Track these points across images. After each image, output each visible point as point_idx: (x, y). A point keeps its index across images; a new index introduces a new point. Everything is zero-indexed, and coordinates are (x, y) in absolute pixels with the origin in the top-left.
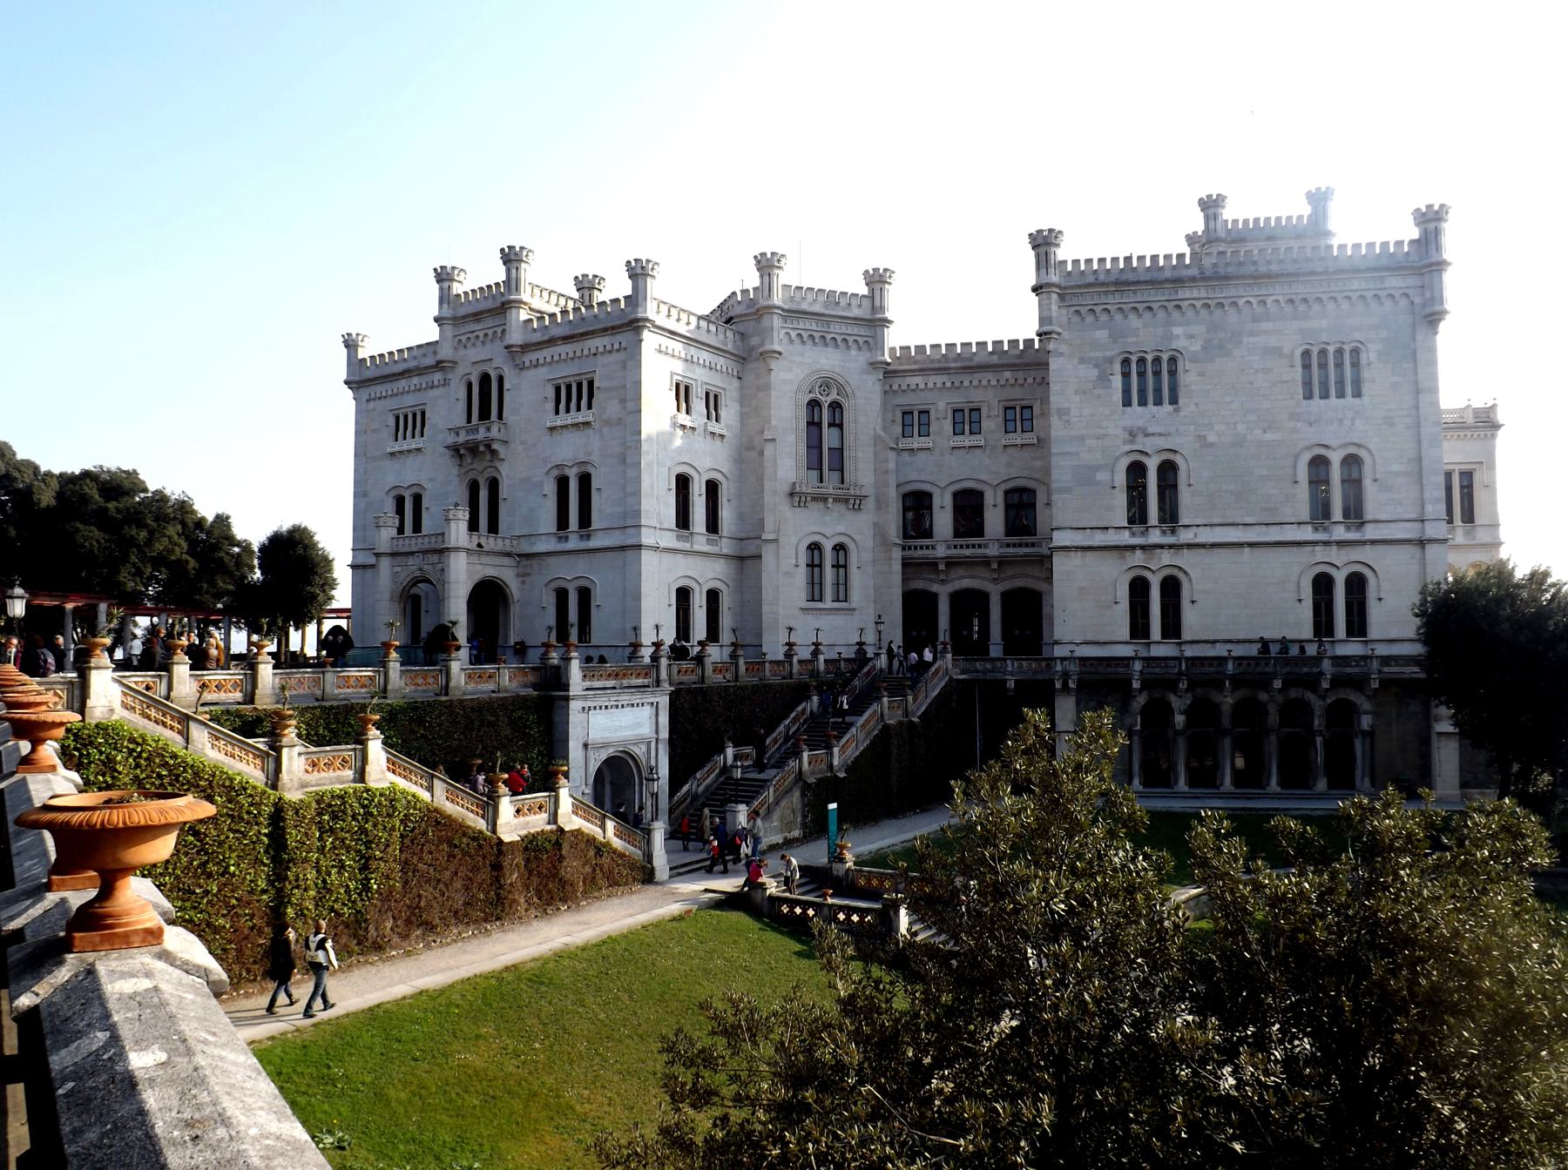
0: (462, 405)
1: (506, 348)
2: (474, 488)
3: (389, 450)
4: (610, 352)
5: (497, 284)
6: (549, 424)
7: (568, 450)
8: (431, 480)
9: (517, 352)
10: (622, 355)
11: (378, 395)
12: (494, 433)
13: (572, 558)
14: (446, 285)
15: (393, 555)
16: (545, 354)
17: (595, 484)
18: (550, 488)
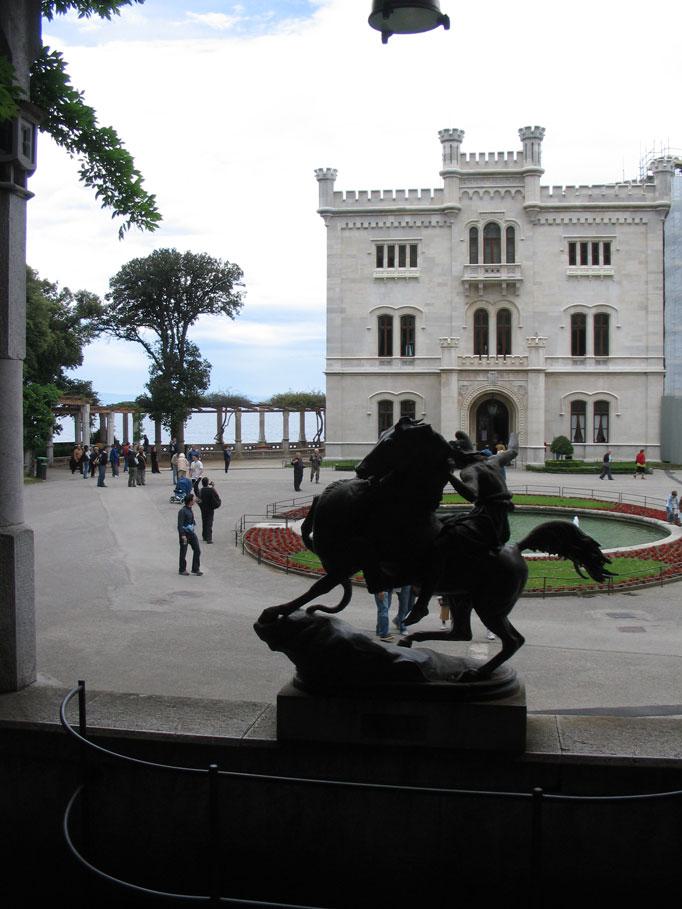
0: (465, 247)
1: (525, 208)
2: (481, 317)
3: (375, 276)
4: (630, 224)
5: (510, 153)
6: (568, 273)
7: (589, 298)
8: (427, 305)
9: (529, 211)
10: (642, 229)
11: (359, 225)
12: (518, 276)
13: (592, 379)
14: (455, 144)
15: (461, 371)
16: (566, 217)
17: (613, 323)
18: (567, 323)
